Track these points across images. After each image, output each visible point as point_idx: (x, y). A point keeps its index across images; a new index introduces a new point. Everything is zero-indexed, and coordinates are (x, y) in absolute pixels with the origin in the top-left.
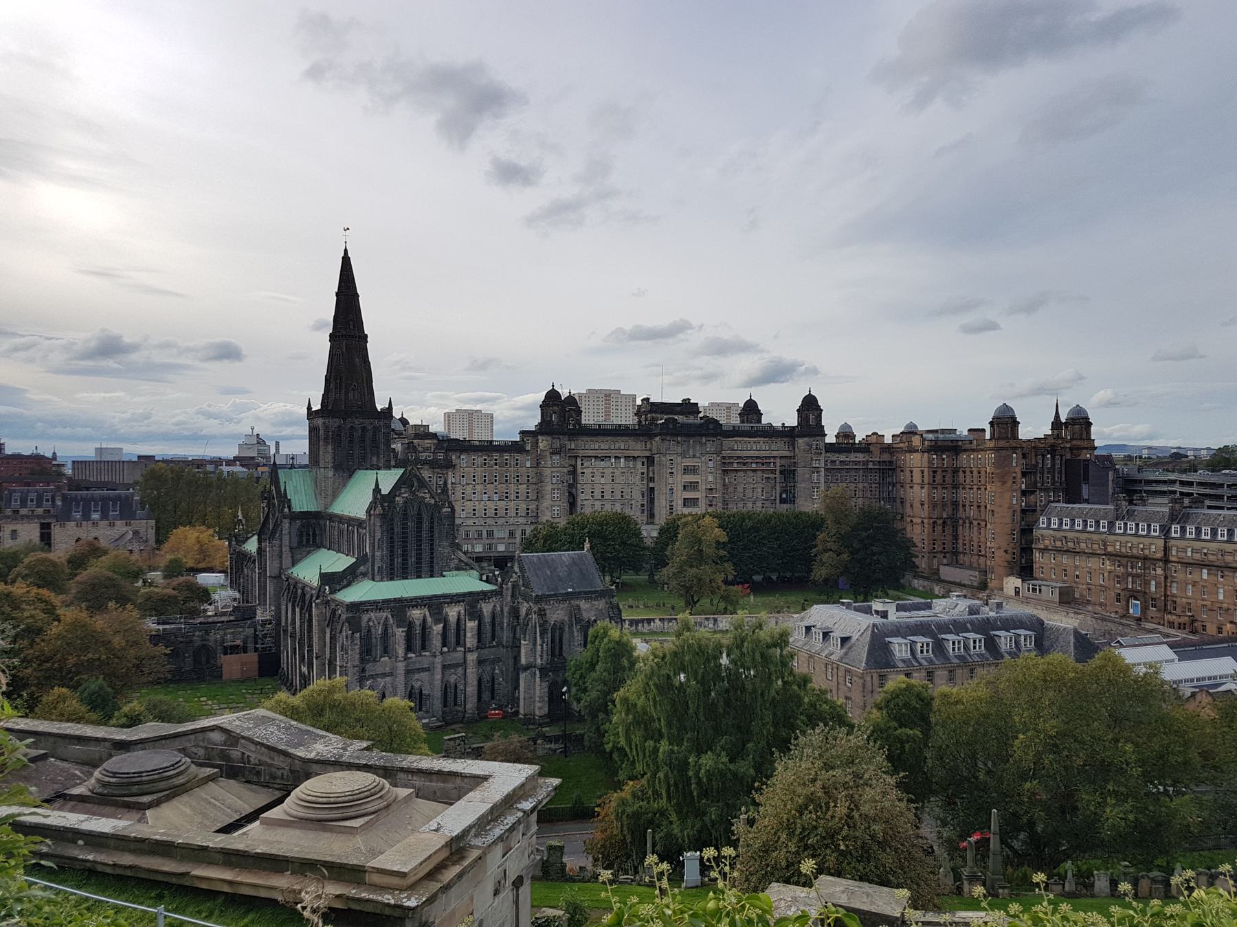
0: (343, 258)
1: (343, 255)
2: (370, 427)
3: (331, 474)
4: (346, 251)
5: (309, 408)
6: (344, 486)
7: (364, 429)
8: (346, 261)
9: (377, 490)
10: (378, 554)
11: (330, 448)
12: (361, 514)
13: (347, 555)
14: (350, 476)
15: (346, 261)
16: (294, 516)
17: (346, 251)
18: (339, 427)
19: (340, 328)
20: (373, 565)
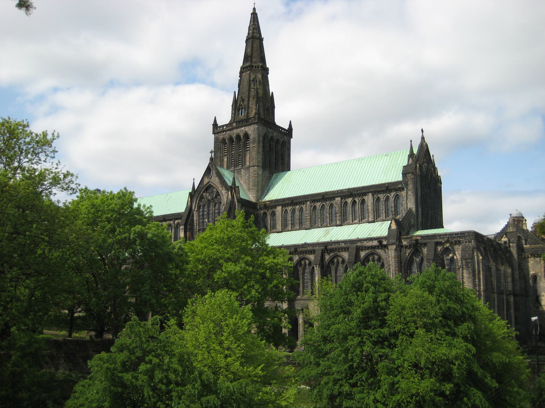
0: (252, 14)
1: (252, 12)
2: (281, 140)
3: (261, 172)
4: (254, 9)
5: (215, 125)
6: (267, 185)
7: (278, 140)
8: (254, 15)
9: (411, 155)
10: (420, 210)
11: (261, 150)
12: (396, 176)
13: (341, 225)
14: (270, 179)
15: (254, 15)
16: (245, 204)
17: (254, 9)
18: (265, 134)
19: (255, 61)
20: (417, 218)
